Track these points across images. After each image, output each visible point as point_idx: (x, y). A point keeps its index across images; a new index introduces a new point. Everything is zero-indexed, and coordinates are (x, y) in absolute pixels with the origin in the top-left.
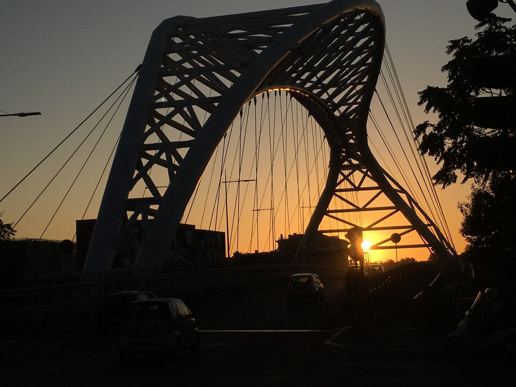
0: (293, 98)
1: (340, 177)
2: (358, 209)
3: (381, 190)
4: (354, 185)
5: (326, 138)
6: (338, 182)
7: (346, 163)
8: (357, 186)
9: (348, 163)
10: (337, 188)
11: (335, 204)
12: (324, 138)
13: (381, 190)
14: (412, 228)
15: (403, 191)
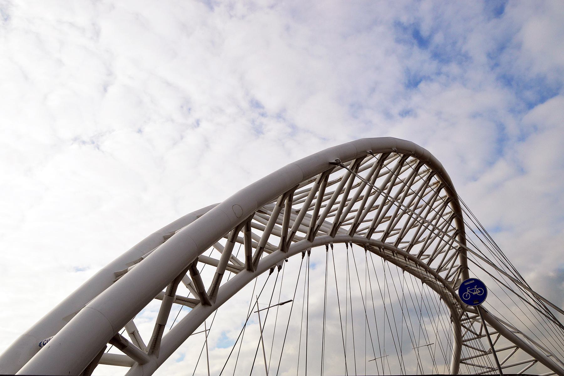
0: (405, 271)
1: (463, 330)
2: (486, 353)
3: (498, 333)
4: (476, 334)
5: (442, 299)
6: (462, 335)
7: (463, 317)
8: (478, 333)
9: (465, 316)
10: (463, 339)
11: (466, 352)
12: (440, 300)
13: (498, 333)
14: (536, 361)
15: (519, 332)
